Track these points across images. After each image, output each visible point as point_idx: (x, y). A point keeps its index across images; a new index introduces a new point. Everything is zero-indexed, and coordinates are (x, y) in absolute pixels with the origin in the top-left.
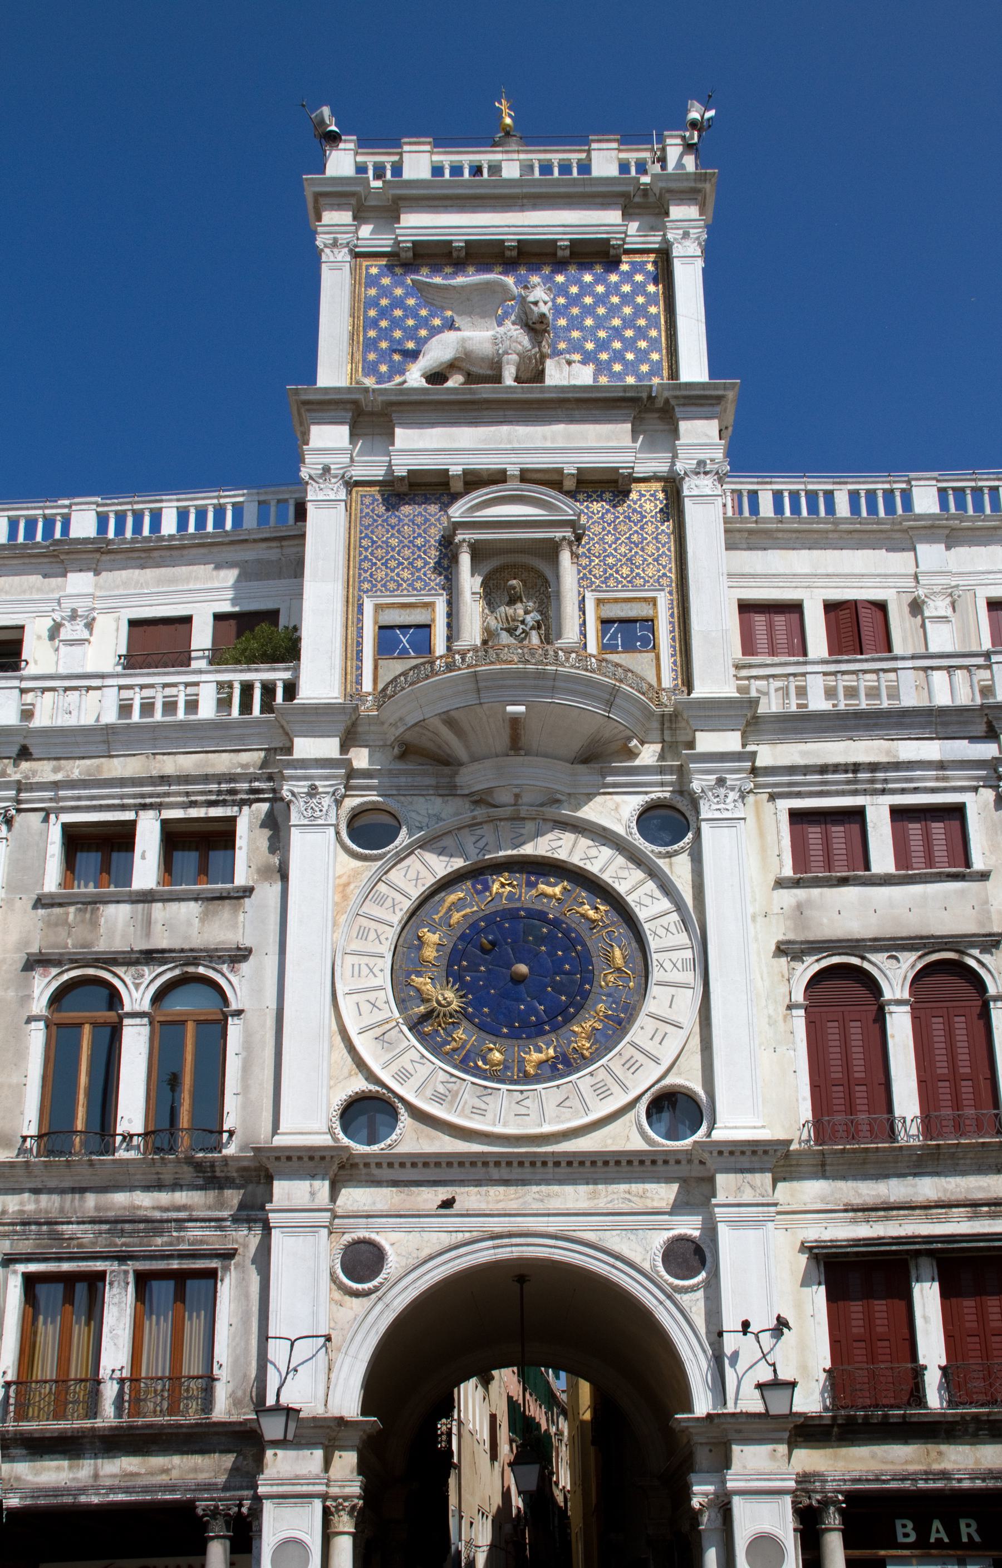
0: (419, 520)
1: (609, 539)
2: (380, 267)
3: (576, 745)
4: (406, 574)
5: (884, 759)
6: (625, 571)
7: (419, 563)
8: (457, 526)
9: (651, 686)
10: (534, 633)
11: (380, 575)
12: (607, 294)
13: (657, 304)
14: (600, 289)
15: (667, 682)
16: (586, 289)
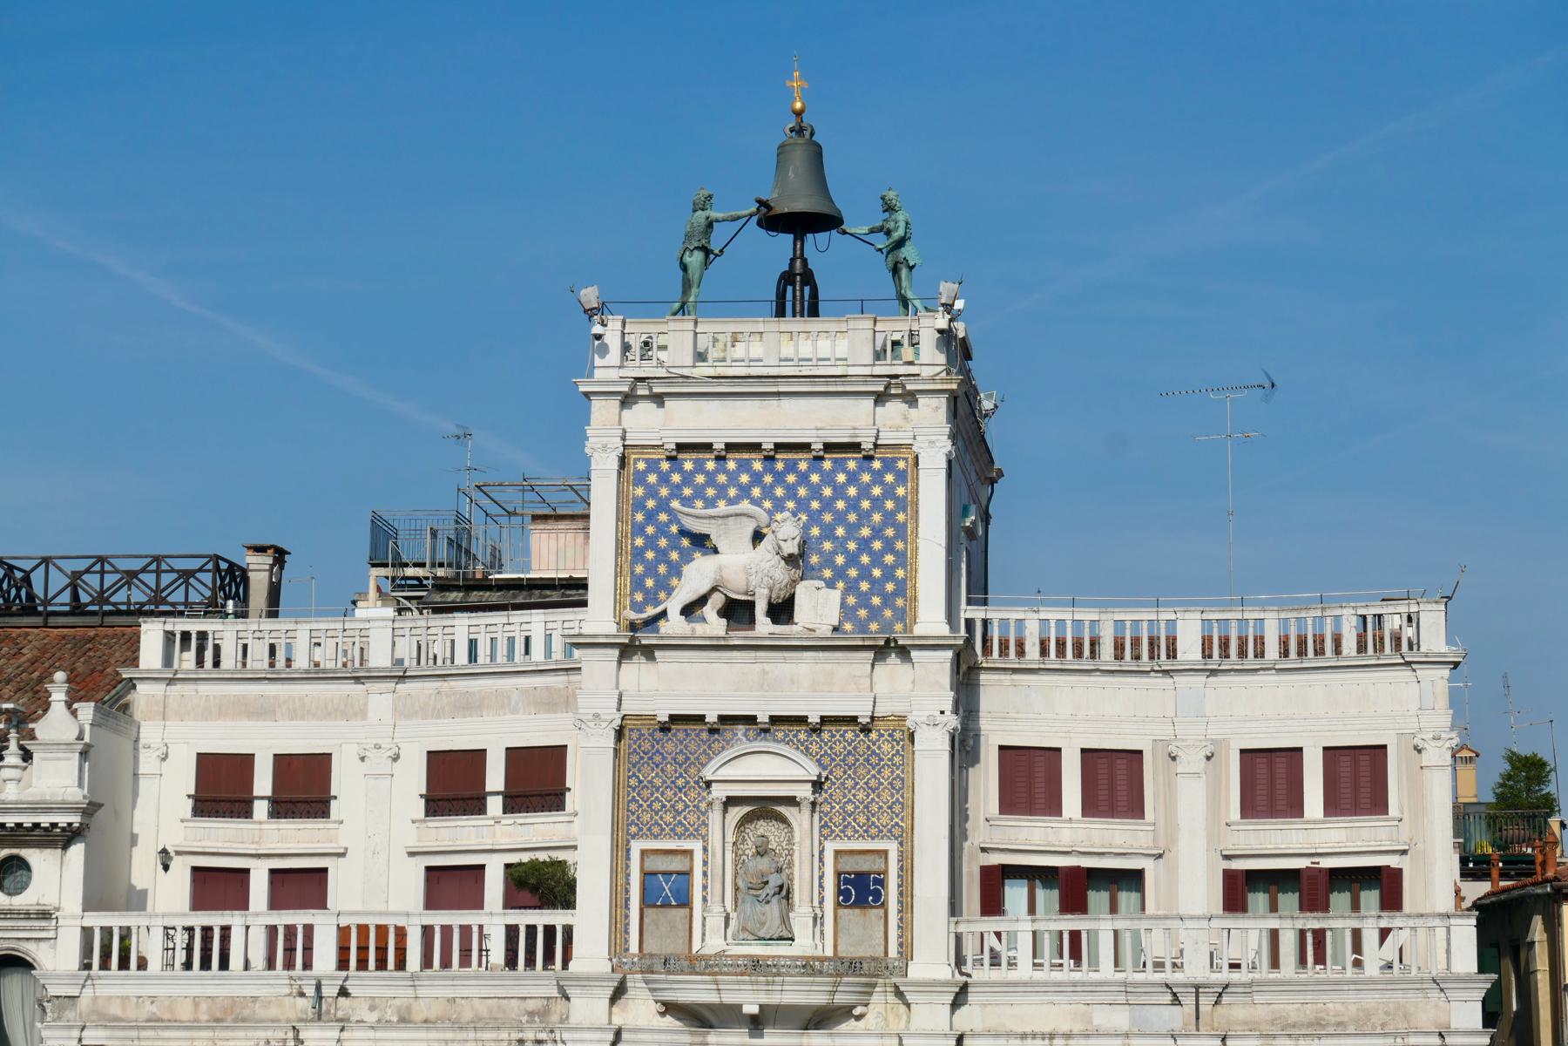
0: (681, 758)
1: (850, 783)
2: (647, 461)
3: (808, 1016)
4: (668, 818)
5: (1077, 1028)
6: (862, 819)
7: (680, 806)
8: (708, 784)
9: (874, 959)
10: (775, 900)
11: (646, 817)
12: (858, 499)
13: (905, 511)
14: (852, 491)
15: (893, 952)
16: (839, 492)
